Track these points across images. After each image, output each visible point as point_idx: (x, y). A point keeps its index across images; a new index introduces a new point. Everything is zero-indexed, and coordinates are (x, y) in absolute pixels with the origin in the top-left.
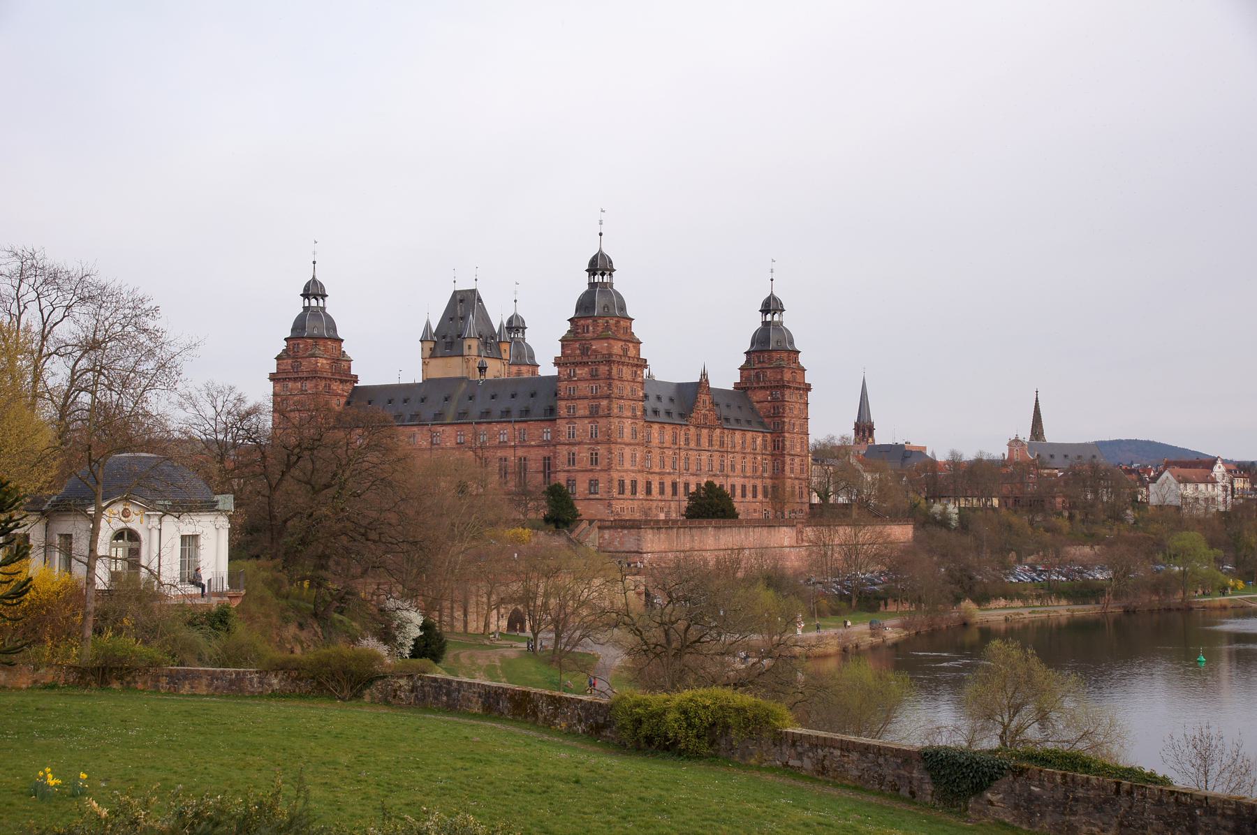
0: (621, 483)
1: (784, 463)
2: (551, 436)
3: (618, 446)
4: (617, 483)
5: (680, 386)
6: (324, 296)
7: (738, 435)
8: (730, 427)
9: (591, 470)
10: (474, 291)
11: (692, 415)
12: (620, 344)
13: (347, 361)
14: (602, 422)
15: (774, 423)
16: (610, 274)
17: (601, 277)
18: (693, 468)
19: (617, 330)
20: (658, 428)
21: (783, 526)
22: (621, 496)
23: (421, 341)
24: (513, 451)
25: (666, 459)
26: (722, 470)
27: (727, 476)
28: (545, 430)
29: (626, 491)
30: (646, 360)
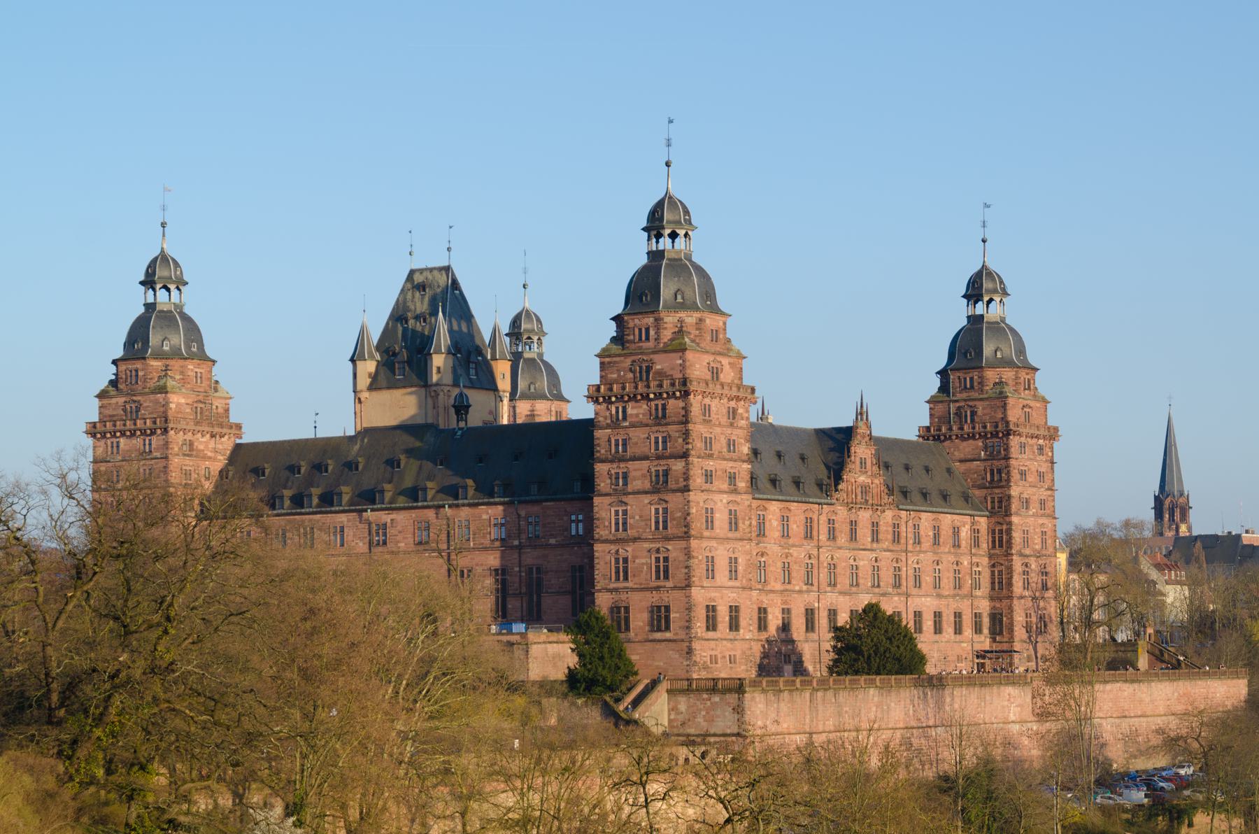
0: (711, 610)
1: (1010, 570)
2: (585, 528)
3: (705, 544)
4: (704, 611)
5: (822, 433)
6: (181, 283)
7: (926, 520)
8: (911, 507)
9: (657, 588)
10: (447, 269)
11: (840, 487)
12: (708, 358)
13: (221, 398)
14: (674, 500)
15: (993, 499)
16: (686, 235)
17: (669, 241)
18: (844, 581)
19: (700, 336)
20: (777, 511)
21: (1007, 684)
22: (711, 634)
23: (353, 360)
24: (516, 556)
25: (794, 567)
26: (897, 585)
27: (908, 595)
28: (573, 517)
30: (753, 390)
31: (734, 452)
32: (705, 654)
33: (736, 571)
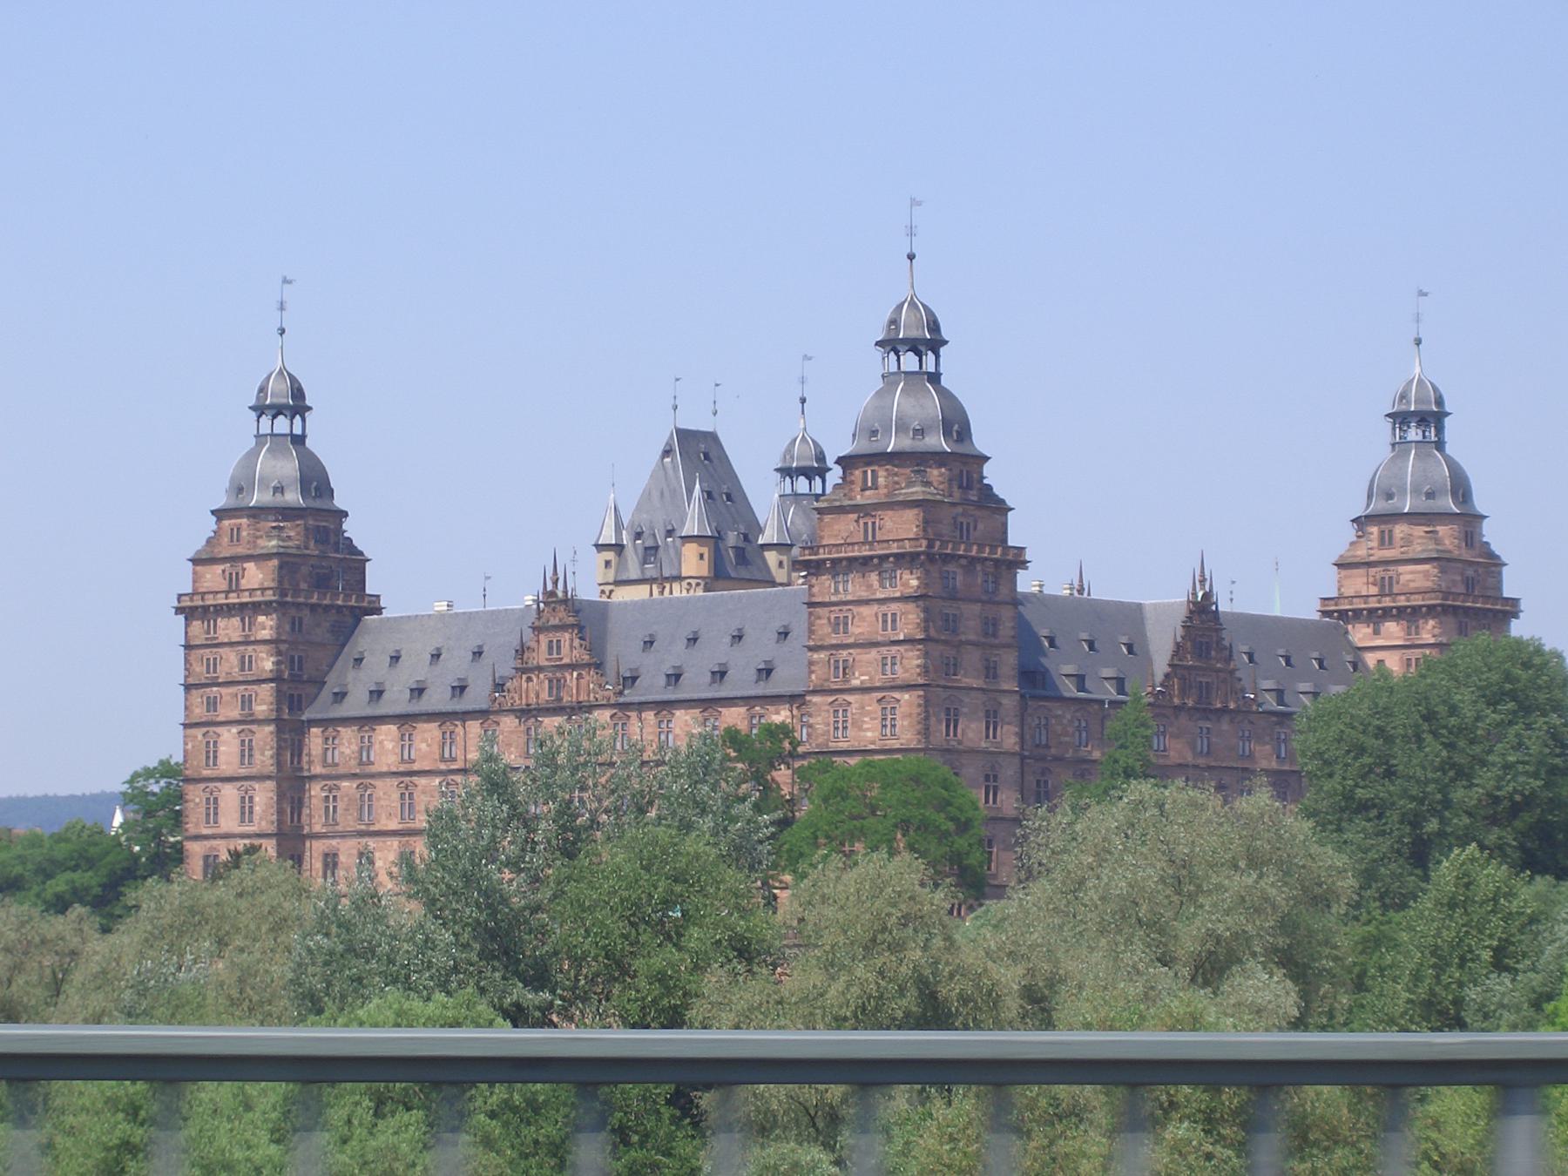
3: (202, 786)
12: (219, 568)
31: (250, 669)
33: (251, 812)
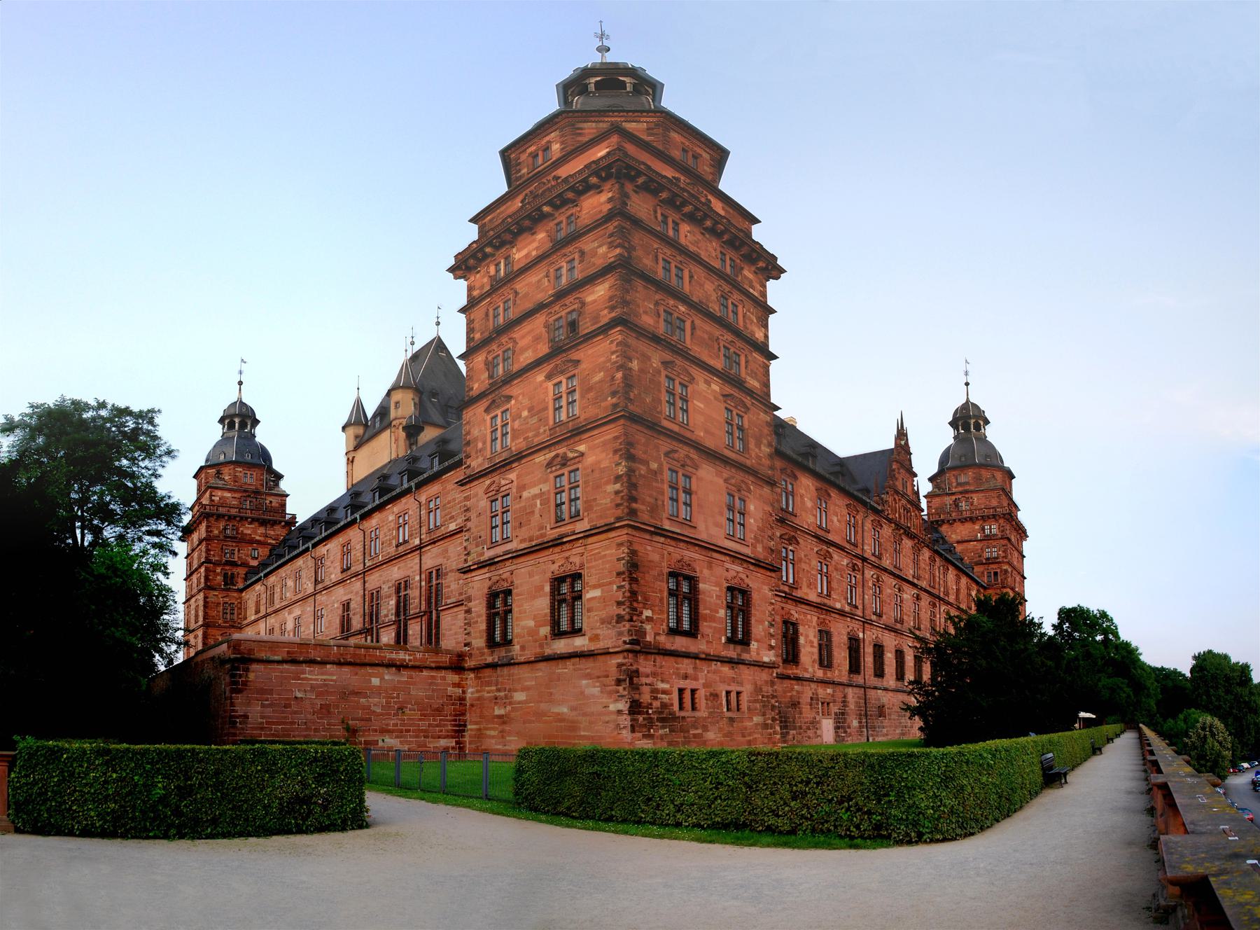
3: (665, 445)
9: (557, 543)
22: (680, 643)
29: (705, 627)
32: (665, 686)
